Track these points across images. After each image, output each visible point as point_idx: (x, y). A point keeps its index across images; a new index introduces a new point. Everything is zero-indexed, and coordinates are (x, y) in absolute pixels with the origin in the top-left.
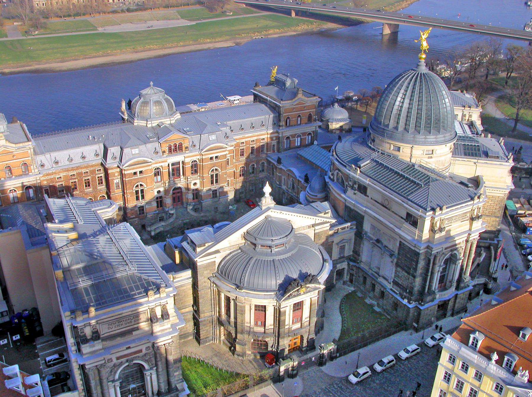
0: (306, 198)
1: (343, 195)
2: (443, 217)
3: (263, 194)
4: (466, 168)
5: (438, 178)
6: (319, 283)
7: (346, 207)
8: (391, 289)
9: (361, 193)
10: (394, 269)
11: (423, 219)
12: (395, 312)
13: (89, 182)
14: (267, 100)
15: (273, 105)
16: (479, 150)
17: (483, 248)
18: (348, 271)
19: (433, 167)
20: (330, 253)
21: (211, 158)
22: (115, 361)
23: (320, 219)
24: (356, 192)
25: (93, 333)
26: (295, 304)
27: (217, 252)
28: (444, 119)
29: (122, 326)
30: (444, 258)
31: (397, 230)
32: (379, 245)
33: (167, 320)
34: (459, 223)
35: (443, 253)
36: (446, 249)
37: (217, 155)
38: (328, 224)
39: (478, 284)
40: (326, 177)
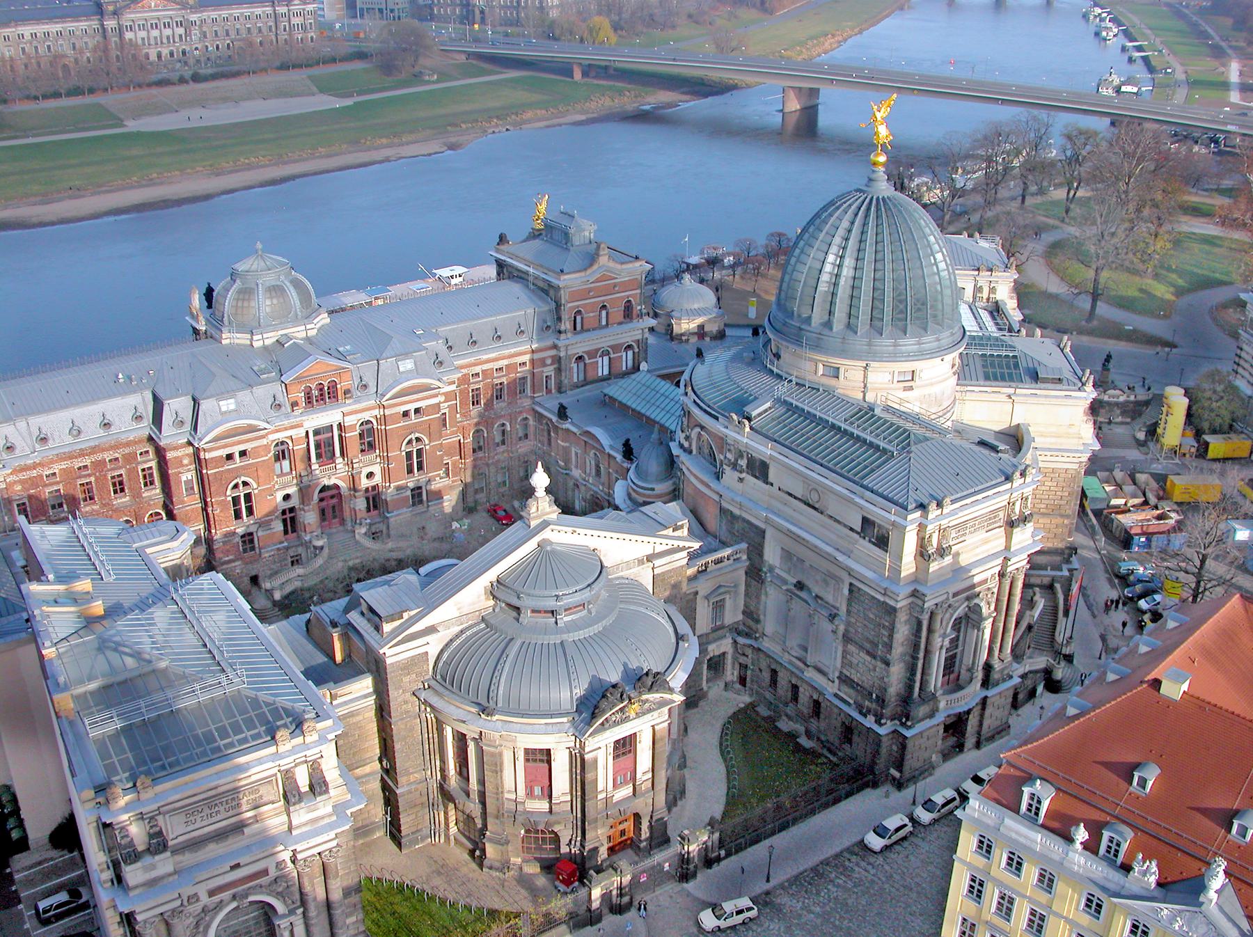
0: (629, 495)
2: (944, 523)
3: (529, 492)
4: (988, 409)
5: (928, 434)
6: (671, 690)
8: (836, 695)
9: (756, 477)
10: (840, 649)
12: (847, 746)
13: (121, 483)
14: (527, 273)
15: (541, 284)
16: (1016, 366)
17: (1037, 589)
18: (735, 659)
19: (917, 410)
20: (691, 619)
21: (406, 414)
22: (205, 899)
23: (664, 541)
24: (744, 475)
25: (151, 836)
26: (617, 742)
27: (432, 630)
28: (936, 301)
29: (219, 817)
30: (952, 615)
31: (841, 558)
32: (803, 594)
33: (324, 797)
34: (981, 535)
35: (950, 606)
36: (955, 595)
37: (417, 405)
38: (684, 554)
39: (1031, 672)
40: (672, 444)
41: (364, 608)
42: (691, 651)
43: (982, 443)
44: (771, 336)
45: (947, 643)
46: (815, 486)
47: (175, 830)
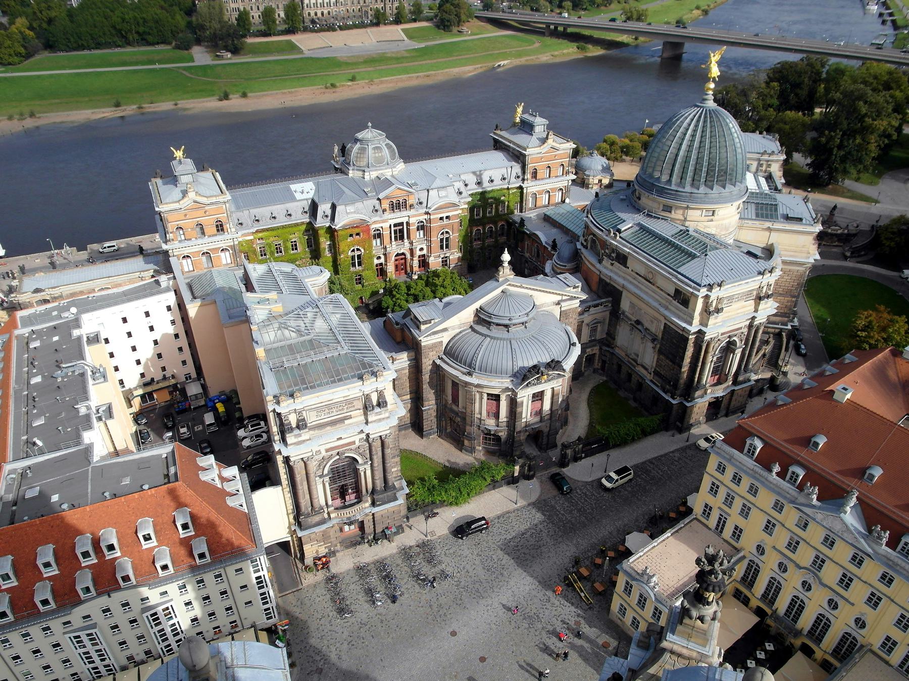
1: (598, 265)
3: (500, 263)
4: (756, 235)
5: (718, 246)
6: (564, 370)
8: (651, 381)
11: (697, 296)
14: (509, 146)
16: (776, 210)
19: (713, 232)
21: (441, 219)
22: (324, 453)
27: (445, 330)
31: (662, 310)
32: (639, 327)
34: (742, 303)
36: (722, 334)
37: (447, 214)
41: (412, 316)
42: (577, 351)
43: (749, 253)
44: (636, 187)
45: (715, 359)
47: (312, 419)
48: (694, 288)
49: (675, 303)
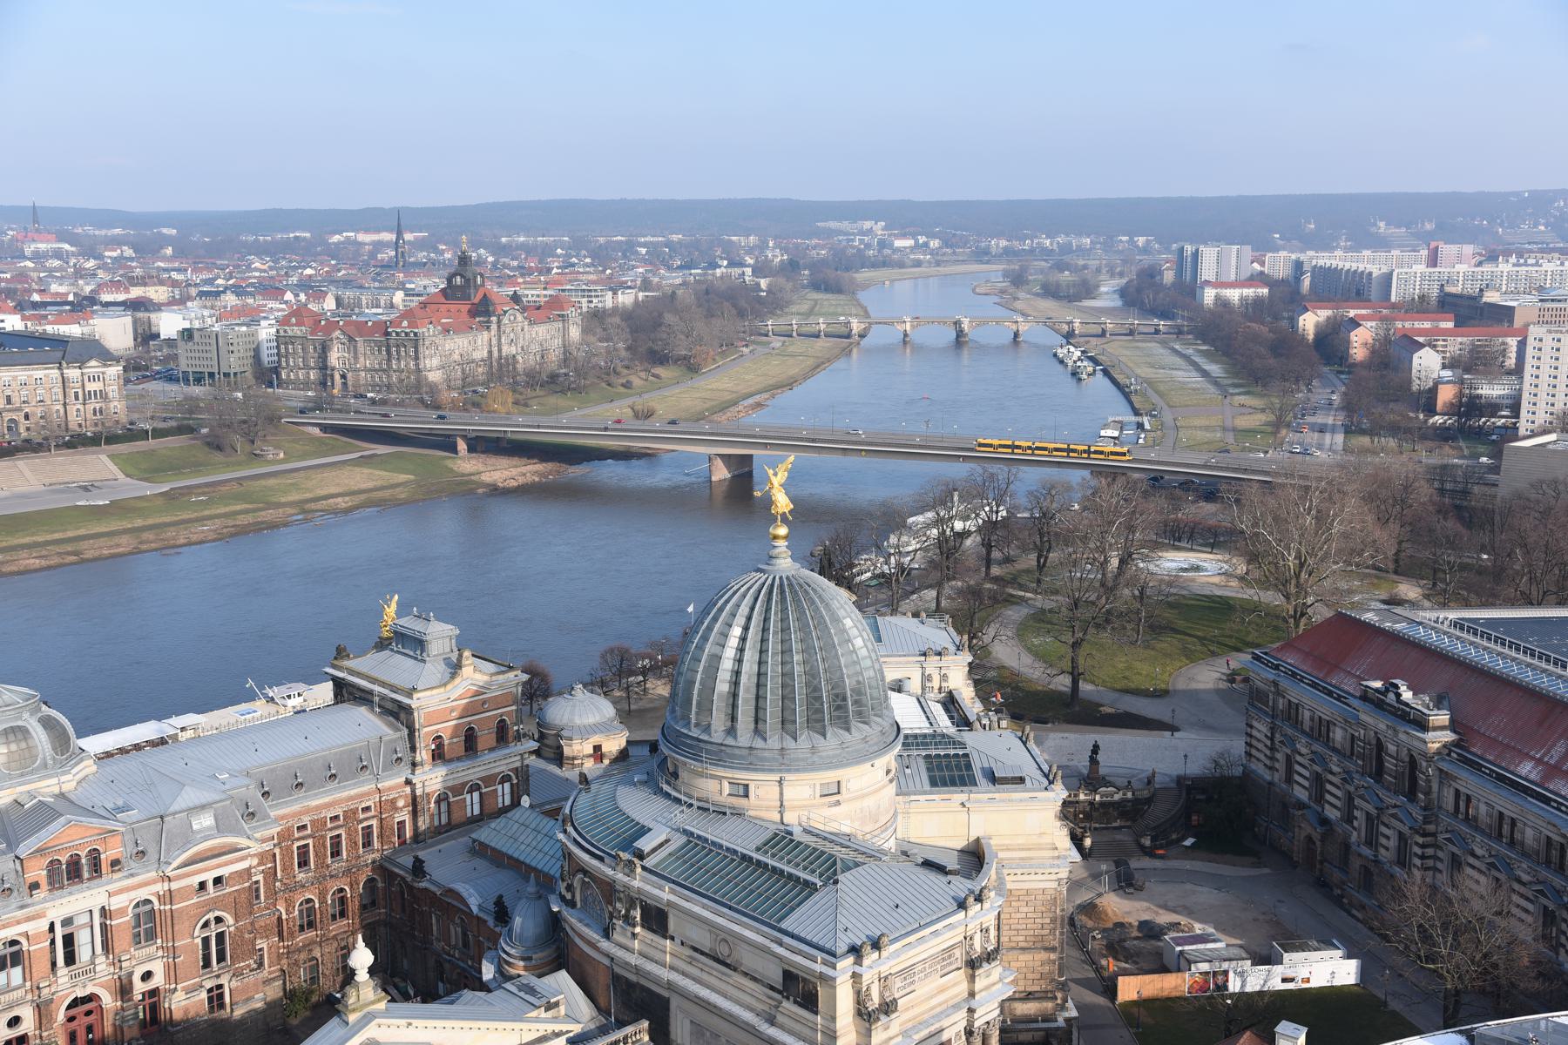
1: (604, 944)
2: (885, 969)
3: (349, 975)
4: (942, 822)
5: (860, 859)
7: (616, 978)
11: (830, 981)
14: (371, 693)
15: (389, 705)
16: (969, 766)
37: (217, 873)
43: (928, 864)
46: (724, 935)
48: (825, 963)
49: (788, 1006)
